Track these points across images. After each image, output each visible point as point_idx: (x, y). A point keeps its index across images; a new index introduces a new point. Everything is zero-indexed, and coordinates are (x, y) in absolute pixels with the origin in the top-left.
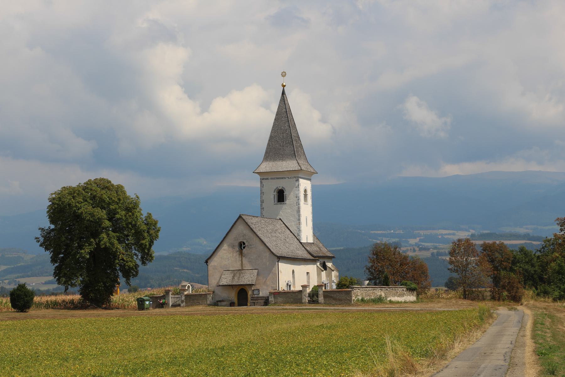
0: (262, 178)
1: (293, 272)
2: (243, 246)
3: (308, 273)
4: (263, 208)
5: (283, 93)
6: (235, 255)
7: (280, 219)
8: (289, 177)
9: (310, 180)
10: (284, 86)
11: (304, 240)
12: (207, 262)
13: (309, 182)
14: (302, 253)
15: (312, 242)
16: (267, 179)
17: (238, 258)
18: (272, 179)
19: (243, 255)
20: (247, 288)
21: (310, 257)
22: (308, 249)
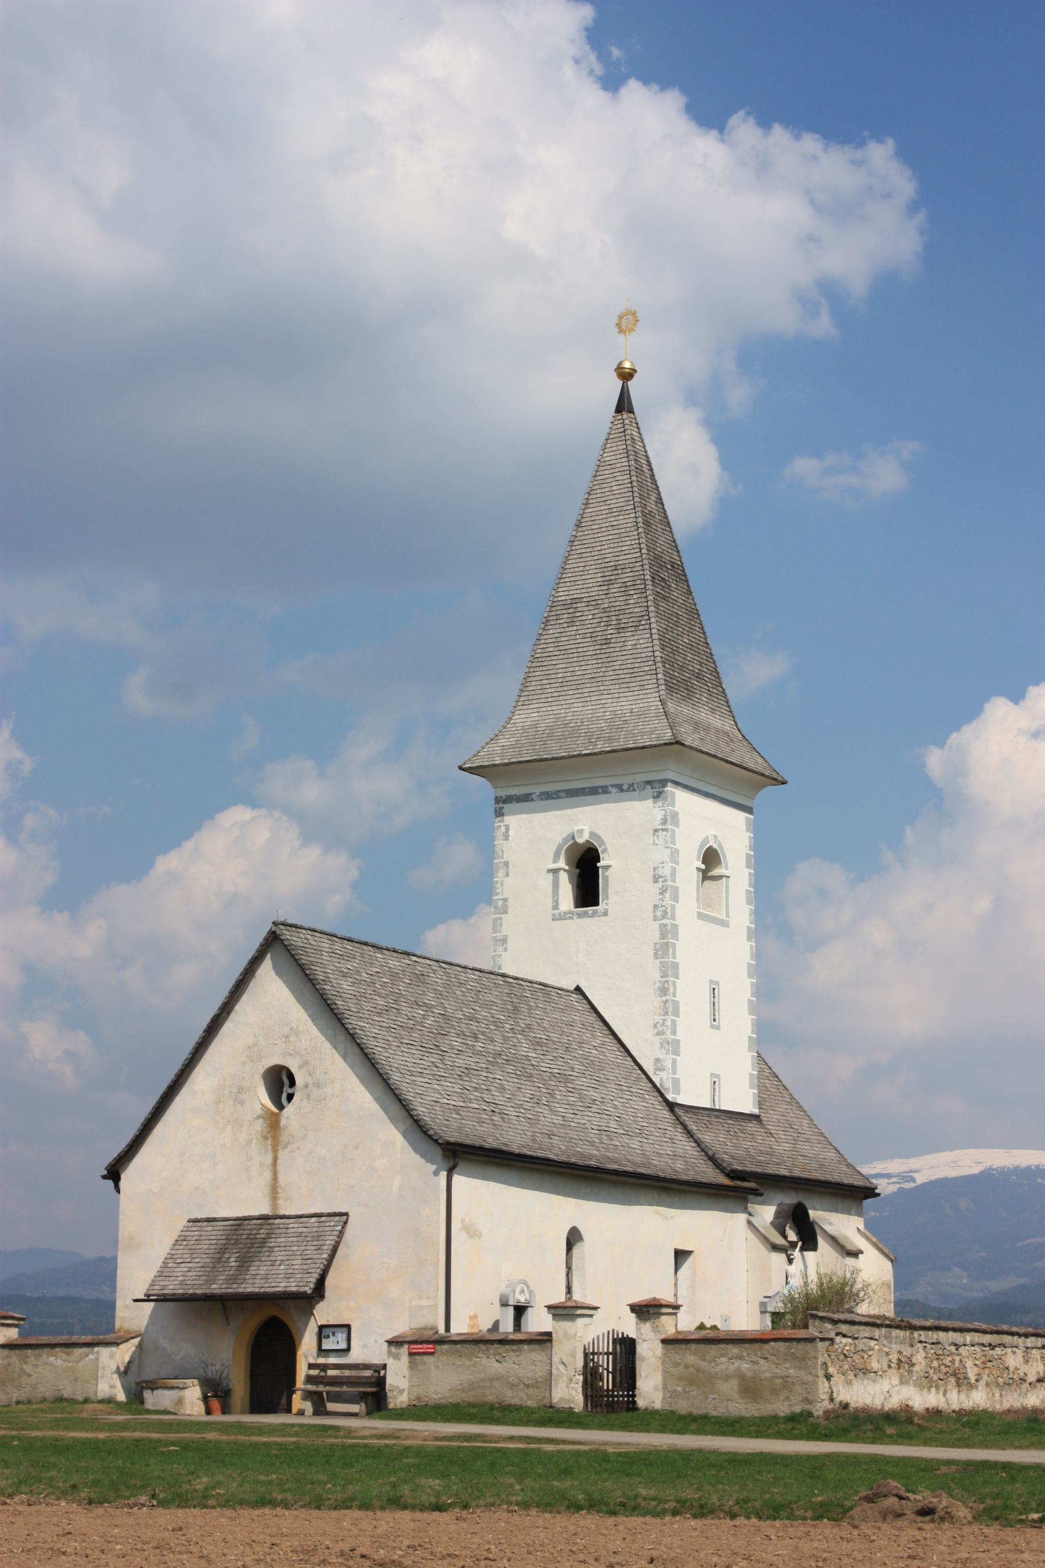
0: (503, 793)
1: (573, 1238)
2: (287, 1090)
3: (681, 1256)
4: (504, 940)
5: (624, 405)
6: (243, 1136)
7: (578, 990)
8: (625, 781)
9: (749, 810)
10: (626, 376)
11: (692, 1093)
12: (114, 1173)
13: (739, 818)
14: (672, 1153)
15: (747, 1105)
16: (526, 798)
17: (261, 1158)
18: (547, 796)
19: (284, 1137)
20: (291, 1318)
21: (726, 1181)
22: (706, 1138)
